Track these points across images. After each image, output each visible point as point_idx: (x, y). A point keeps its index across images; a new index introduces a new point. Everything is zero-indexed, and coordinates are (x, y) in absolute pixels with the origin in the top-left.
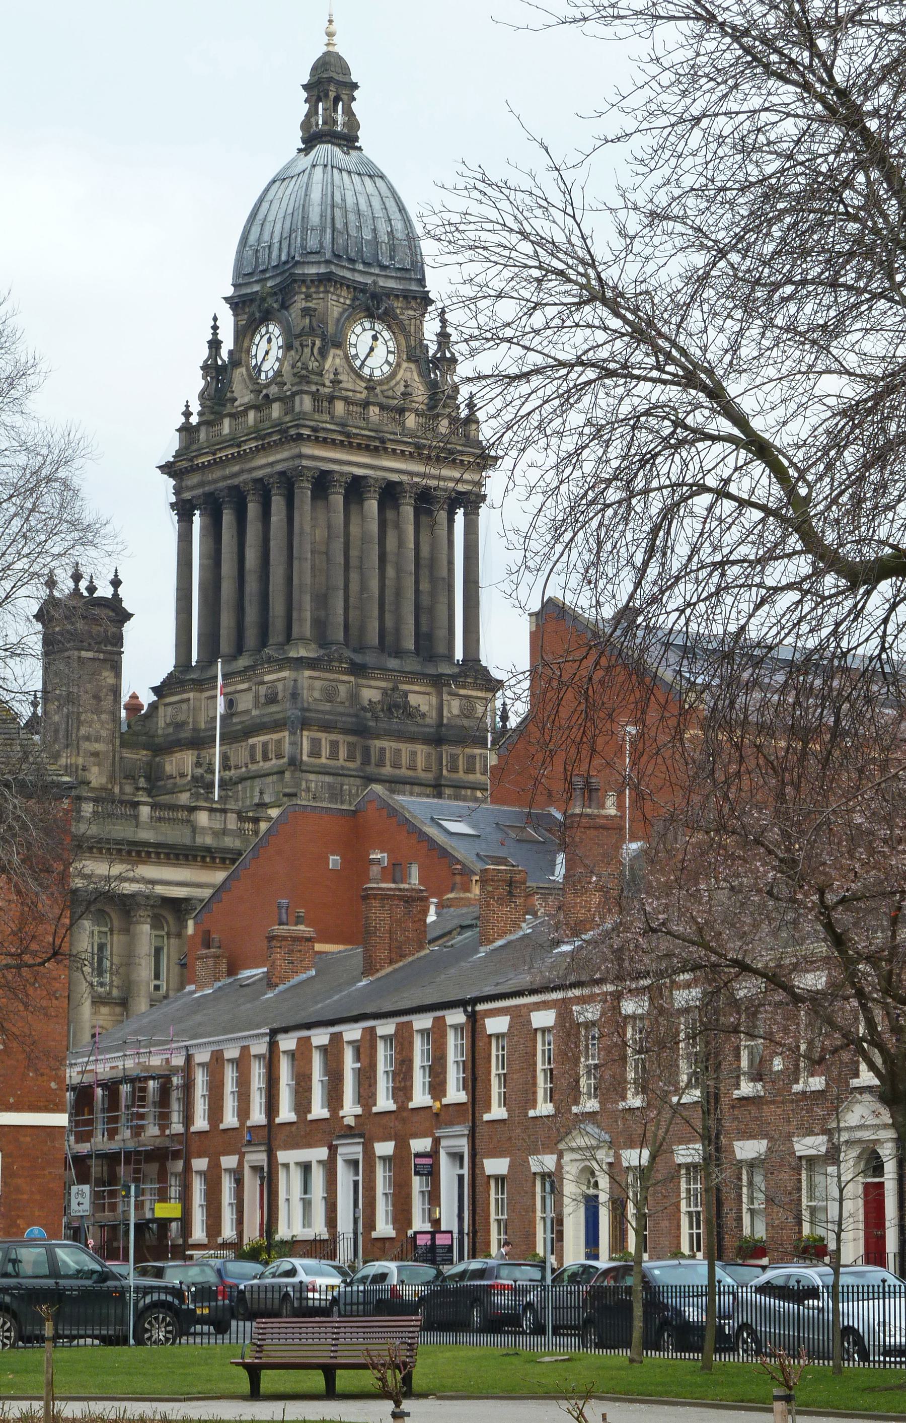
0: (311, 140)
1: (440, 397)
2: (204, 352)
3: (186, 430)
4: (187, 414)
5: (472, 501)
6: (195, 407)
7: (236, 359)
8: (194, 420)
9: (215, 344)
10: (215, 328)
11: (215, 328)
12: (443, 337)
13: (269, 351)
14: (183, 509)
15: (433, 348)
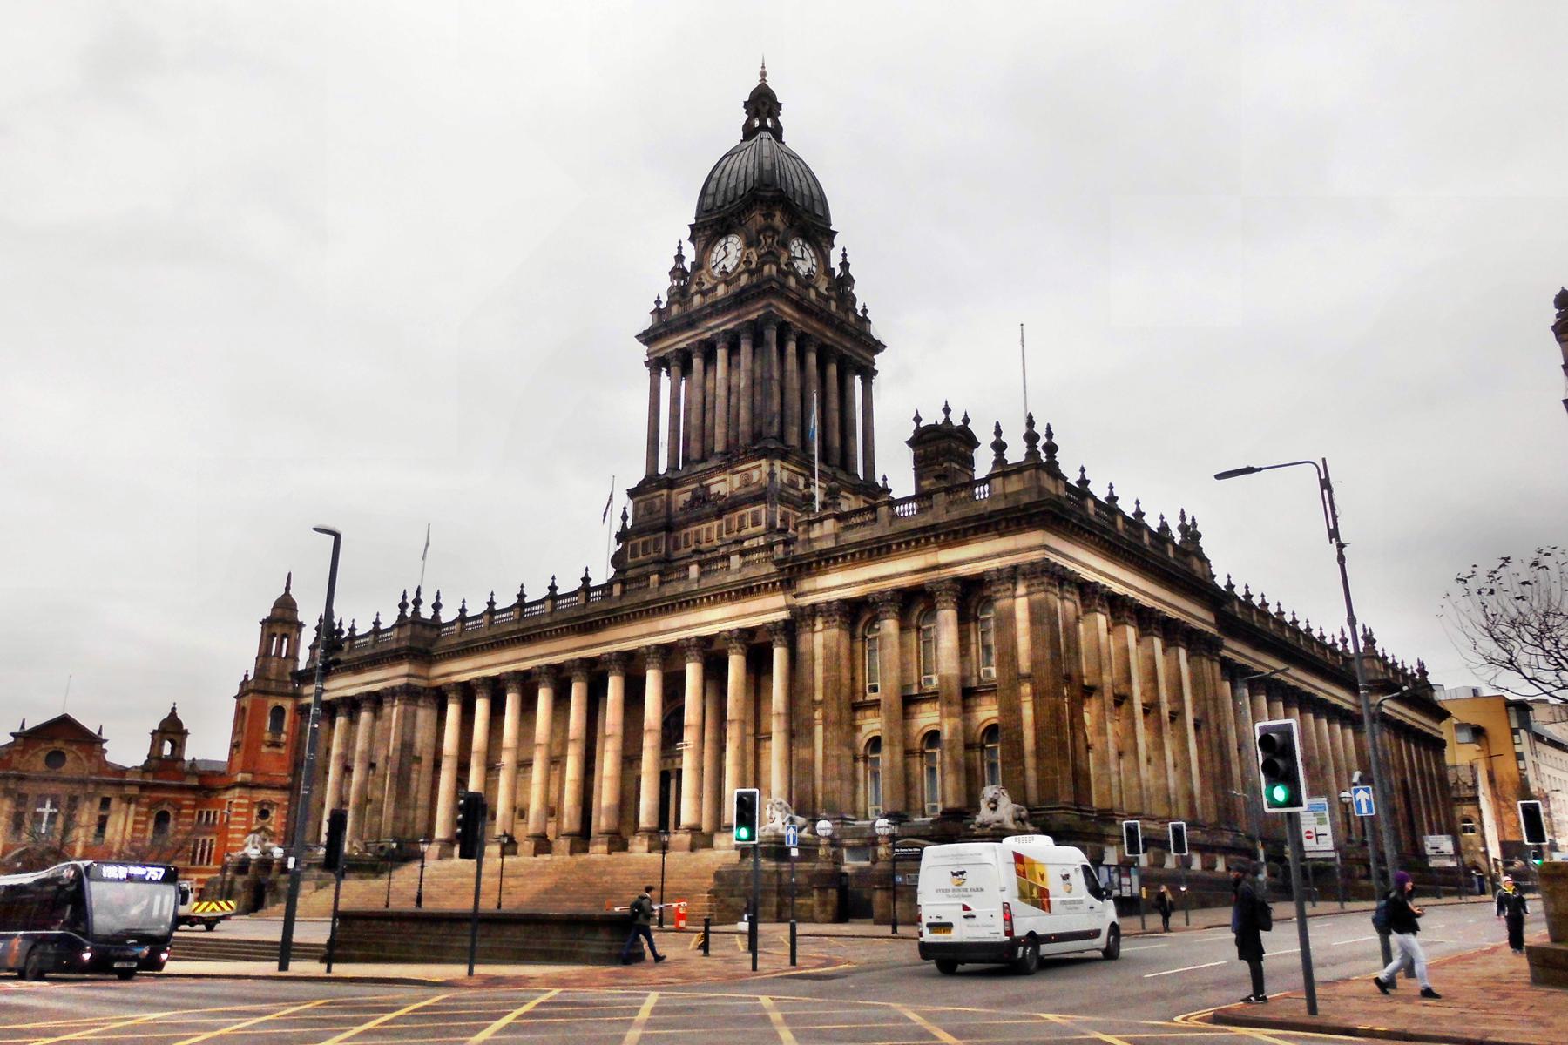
0: (749, 132)
1: (847, 300)
2: (672, 263)
3: (658, 312)
4: (658, 302)
5: (868, 374)
6: (665, 300)
7: (698, 266)
8: (663, 306)
9: (680, 258)
10: (680, 248)
11: (680, 248)
12: (845, 265)
13: (730, 253)
14: (656, 365)
15: (838, 272)
